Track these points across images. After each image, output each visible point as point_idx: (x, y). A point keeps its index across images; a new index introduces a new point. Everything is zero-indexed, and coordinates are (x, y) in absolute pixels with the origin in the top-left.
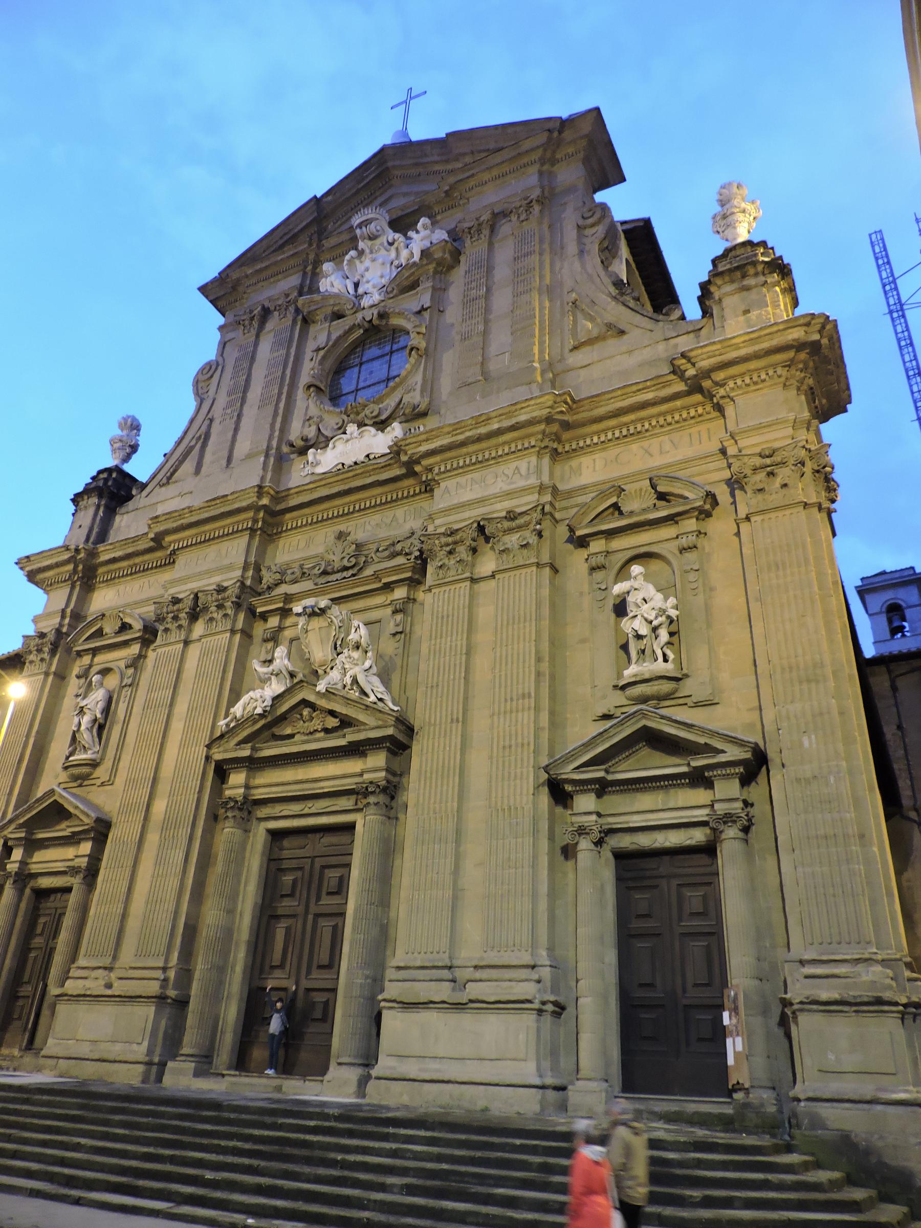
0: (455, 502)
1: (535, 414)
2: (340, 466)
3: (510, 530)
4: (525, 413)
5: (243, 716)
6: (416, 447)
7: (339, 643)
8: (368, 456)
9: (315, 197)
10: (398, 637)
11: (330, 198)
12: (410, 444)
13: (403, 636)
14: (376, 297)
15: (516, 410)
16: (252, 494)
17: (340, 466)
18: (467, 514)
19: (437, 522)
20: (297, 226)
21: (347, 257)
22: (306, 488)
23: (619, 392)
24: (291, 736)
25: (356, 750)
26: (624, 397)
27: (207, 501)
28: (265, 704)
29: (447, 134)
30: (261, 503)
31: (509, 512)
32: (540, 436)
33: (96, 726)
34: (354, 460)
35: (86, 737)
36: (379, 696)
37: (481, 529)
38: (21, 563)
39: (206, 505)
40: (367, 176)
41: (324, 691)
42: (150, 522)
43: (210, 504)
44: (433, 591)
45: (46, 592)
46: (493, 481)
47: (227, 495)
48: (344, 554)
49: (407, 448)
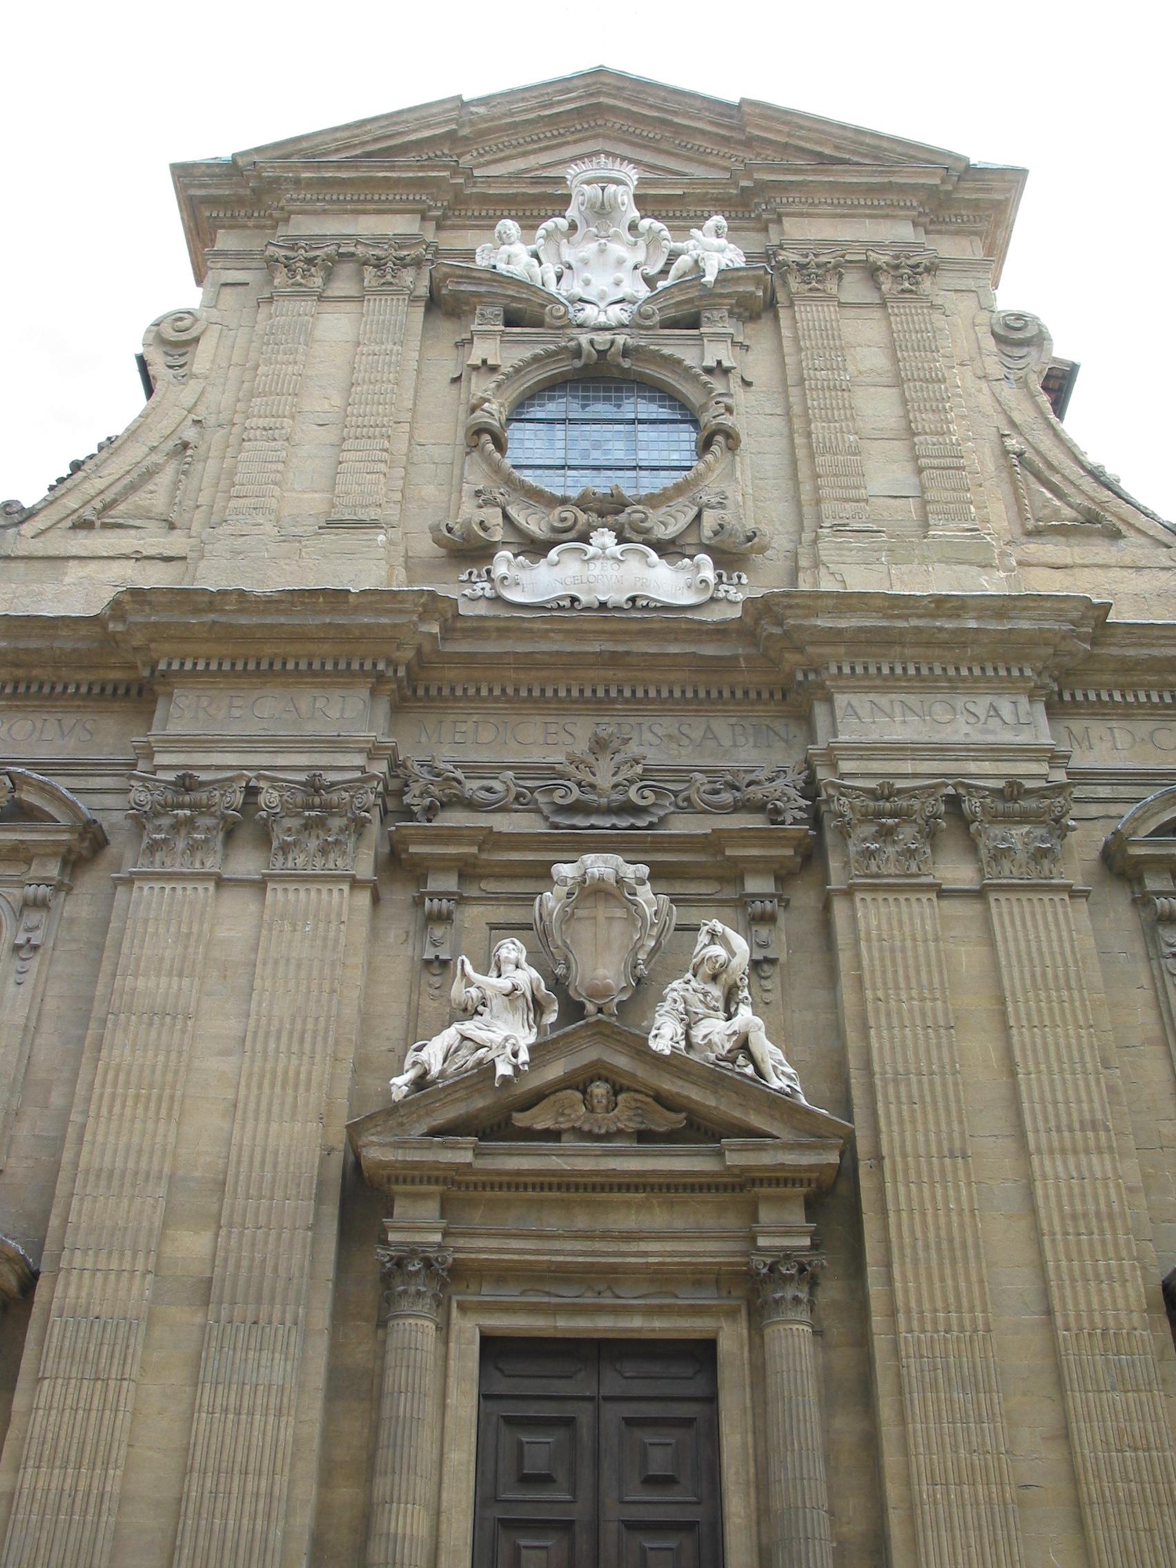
0: (874, 737)
2: (567, 603)
3: (1009, 819)
4: (1029, 619)
5: (442, 1074)
6: (807, 617)
7: (642, 956)
8: (633, 599)
9: (459, 97)
11: (482, 110)
12: (797, 606)
13: (778, 969)
14: (617, 314)
15: (1015, 608)
16: (409, 606)
17: (567, 603)
18: (908, 767)
21: (549, 224)
29: (743, 101)
30: (424, 628)
34: (602, 598)
37: (954, 802)
40: (560, 103)
42: (127, 598)
48: (619, 778)
49: (788, 612)
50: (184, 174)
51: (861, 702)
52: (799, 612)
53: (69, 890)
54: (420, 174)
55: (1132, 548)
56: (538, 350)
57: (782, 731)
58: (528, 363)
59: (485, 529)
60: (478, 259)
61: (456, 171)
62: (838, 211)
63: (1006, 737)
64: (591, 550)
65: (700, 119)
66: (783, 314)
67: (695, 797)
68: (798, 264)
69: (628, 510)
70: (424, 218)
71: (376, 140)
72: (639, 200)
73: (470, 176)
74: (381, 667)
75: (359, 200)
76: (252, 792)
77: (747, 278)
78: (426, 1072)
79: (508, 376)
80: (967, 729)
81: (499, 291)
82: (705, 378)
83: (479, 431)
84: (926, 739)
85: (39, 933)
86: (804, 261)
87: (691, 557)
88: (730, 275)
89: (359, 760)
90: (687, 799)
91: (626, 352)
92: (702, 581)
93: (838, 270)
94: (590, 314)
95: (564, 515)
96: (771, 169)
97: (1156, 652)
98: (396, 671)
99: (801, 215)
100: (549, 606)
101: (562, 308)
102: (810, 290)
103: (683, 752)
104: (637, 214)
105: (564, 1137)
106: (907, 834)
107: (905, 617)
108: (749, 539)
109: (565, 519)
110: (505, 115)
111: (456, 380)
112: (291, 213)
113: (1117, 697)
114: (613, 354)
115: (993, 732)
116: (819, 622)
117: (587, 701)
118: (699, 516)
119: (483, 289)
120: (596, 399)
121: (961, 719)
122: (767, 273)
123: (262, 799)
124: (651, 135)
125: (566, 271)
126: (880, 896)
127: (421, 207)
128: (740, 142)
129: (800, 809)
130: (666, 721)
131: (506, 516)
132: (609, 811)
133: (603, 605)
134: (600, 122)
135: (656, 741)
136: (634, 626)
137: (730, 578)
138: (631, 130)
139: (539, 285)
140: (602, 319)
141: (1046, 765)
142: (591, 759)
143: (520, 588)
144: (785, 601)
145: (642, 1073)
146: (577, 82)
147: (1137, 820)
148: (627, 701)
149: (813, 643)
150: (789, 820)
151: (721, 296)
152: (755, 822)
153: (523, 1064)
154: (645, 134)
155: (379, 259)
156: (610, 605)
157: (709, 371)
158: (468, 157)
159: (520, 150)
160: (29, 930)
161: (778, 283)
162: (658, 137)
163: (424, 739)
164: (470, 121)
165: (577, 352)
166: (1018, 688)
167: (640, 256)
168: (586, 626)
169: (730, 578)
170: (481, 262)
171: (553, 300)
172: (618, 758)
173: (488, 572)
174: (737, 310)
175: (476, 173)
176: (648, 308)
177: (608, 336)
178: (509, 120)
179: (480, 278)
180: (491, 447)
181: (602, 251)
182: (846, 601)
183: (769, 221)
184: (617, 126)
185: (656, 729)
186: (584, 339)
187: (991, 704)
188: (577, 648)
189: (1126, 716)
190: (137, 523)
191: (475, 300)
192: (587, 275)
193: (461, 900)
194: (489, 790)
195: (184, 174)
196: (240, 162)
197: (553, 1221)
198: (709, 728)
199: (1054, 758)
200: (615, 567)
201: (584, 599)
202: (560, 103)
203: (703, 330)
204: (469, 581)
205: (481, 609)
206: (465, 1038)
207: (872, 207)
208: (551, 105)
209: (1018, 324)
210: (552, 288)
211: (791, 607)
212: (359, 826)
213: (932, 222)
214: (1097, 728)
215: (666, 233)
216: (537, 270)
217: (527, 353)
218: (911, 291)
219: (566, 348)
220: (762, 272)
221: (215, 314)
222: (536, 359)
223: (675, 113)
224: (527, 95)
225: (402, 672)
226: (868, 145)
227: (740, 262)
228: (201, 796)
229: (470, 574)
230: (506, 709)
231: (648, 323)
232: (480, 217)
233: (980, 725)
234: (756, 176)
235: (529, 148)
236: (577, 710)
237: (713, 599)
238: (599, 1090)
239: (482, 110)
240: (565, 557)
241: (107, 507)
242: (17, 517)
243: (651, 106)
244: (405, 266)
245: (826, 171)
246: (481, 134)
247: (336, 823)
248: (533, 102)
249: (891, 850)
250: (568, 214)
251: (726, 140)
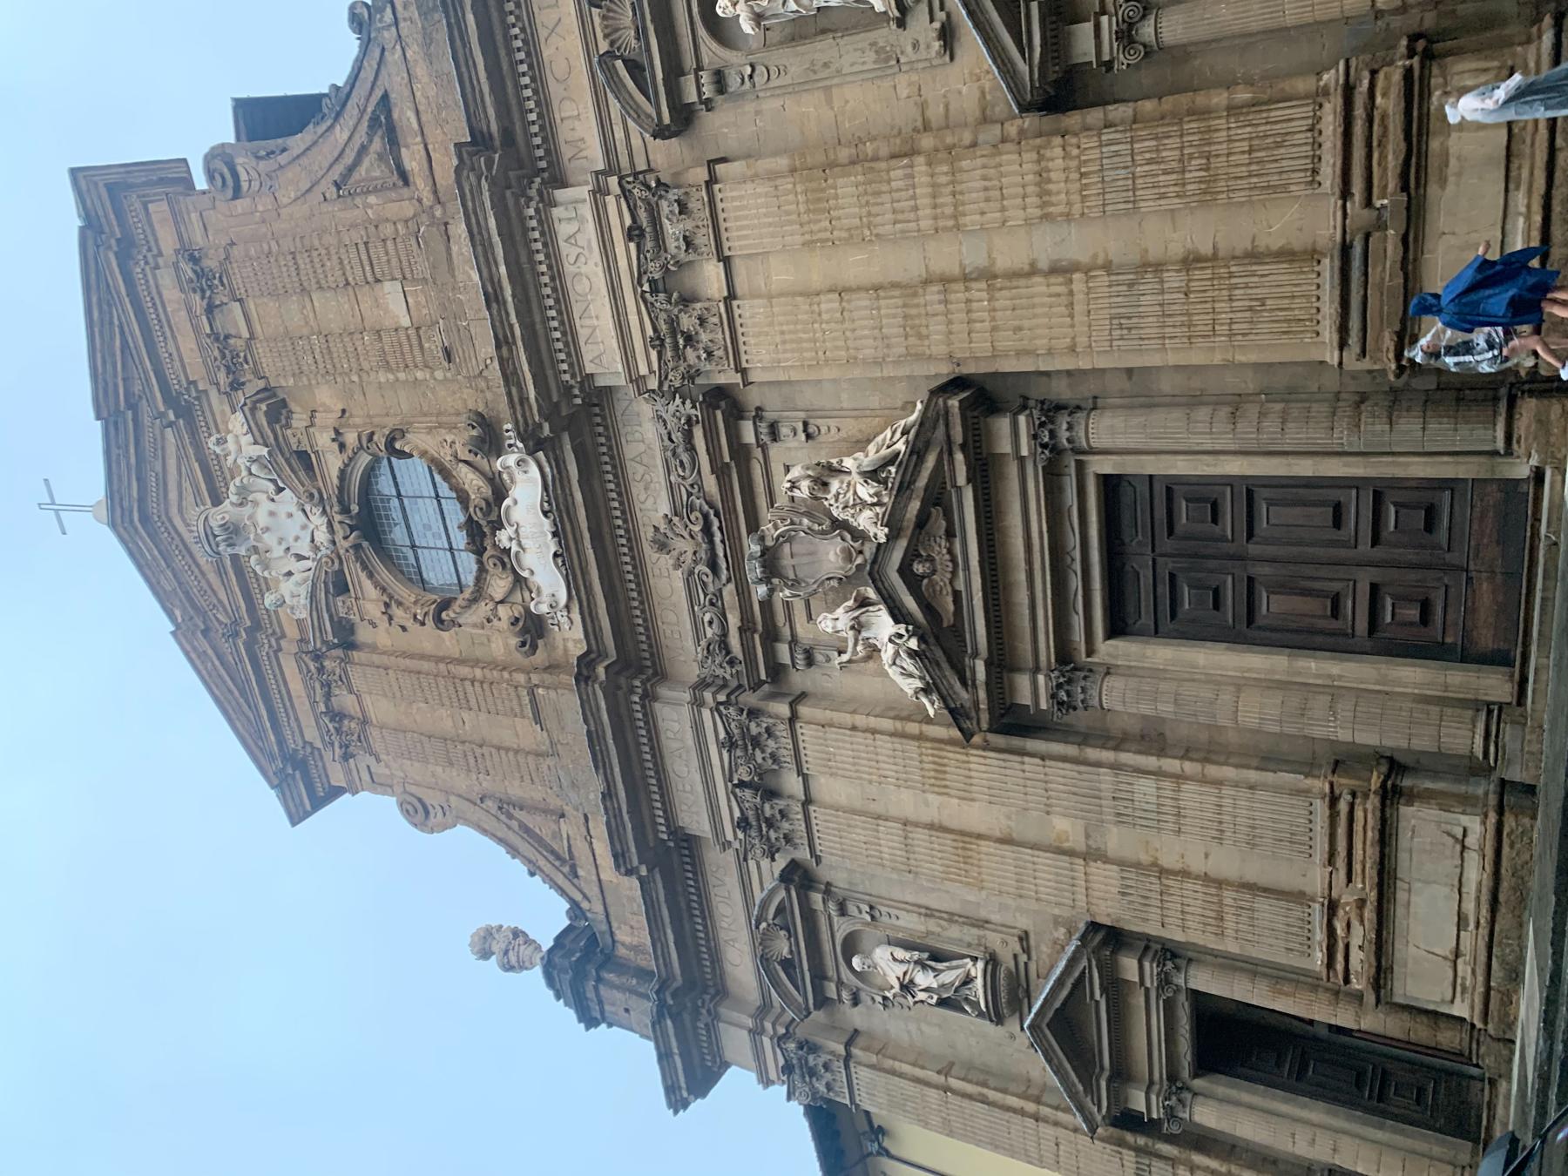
1: (488, 204)
2: (560, 561)
5: (922, 678)
7: (816, 527)
8: (545, 514)
10: (811, 429)
11: (178, 613)
13: (811, 421)
14: (318, 520)
18: (633, 319)
19: (643, 370)
21: (258, 569)
22: (585, 604)
23: (464, 69)
24: (957, 595)
25: (985, 471)
26: (471, 63)
27: (596, 767)
28: (903, 632)
29: (98, 417)
31: (631, 239)
32: (522, 200)
33: (932, 963)
34: (550, 536)
35: (950, 976)
36: (898, 435)
38: (677, 1102)
39: (601, 771)
41: (886, 530)
43: (601, 764)
44: (744, 365)
45: (725, 1065)
46: (585, 280)
47: (589, 732)
50: (297, 816)
51: (588, 353)
53: (828, 884)
55: (394, 80)
56: (363, 576)
57: (625, 404)
59: (517, 620)
62: (168, 334)
63: (590, 227)
64: (515, 548)
67: (690, 481)
68: (228, 374)
72: (217, 501)
74: (636, 699)
76: (742, 784)
78: (922, 689)
79: (391, 597)
80: (591, 263)
81: (323, 602)
84: (607, 299)
85: (862, 906)
89: (706, 713)
90: (692, 486)
91: (345, 510)
93: (221, 339)
94: (322, 536)
97: (486, 89)
103: (655, 480)
104: (227, 501)
105: (958, 588)
106: (687, 322)
107: (511, 326)
112: (305, 742)
113: (533, 117)
115: (589, 241)
120: (387, 517)
121: (584, 269)
123: (746, 778)
125: (293, 551)
126: (742, 348)
127: (272, 654)
129: (683, 403)
130: (635, 491)
132: (711, 542)
133: (555, 534)
135: (651, 500)
140: (324, 528)
141: (608, 198)
142: (675, 553)
145: (902, 544)
147: (638, 115)
149: (550, 398)
150: (693, 412)
151: (276, 438)
152: (698, 433)
153: (907, 631)
160: (860, 912)
163: (682, 659)
165: (357, 547)
166: (547, 218)
167: (262, 497)
170: (303, 614)
172: (670, 534)
174: (284, 422)
177: (337, 526)
181: (267, 529)
182: (510, 376)
183: (197, 391)
185: (642, 499)
187: (566, 241)
189: (548, 104)
190: (565, 836)
191: (336, 619)
192: (291, 539)
193: (794, 641)
194: (711, 623)
195: (297, 816)
196: (276, 782)
197: (1021, 596)
198: (632, 460)
199: (599, 192)
201: (553, 548)
205: (576, 617)
206: (894, 663)
209: (217, 177)
212: (754, 713)
213: (150, 250)
214: (564, 133)
215: (237, 481)
216: (297, 577)
217: (367, 584)
218: (220, 277)
220: (246, 408)
221: (398, 789)
222: (371, 576)
228: (750, 814)
233: (586, 252)
234: (162, 409)
238: (919, 568)
239: (178, 613)
241: (558, 857)
242: (578, 912)
244: (323, 667)
247: (754, 730)
249: (704, 337)
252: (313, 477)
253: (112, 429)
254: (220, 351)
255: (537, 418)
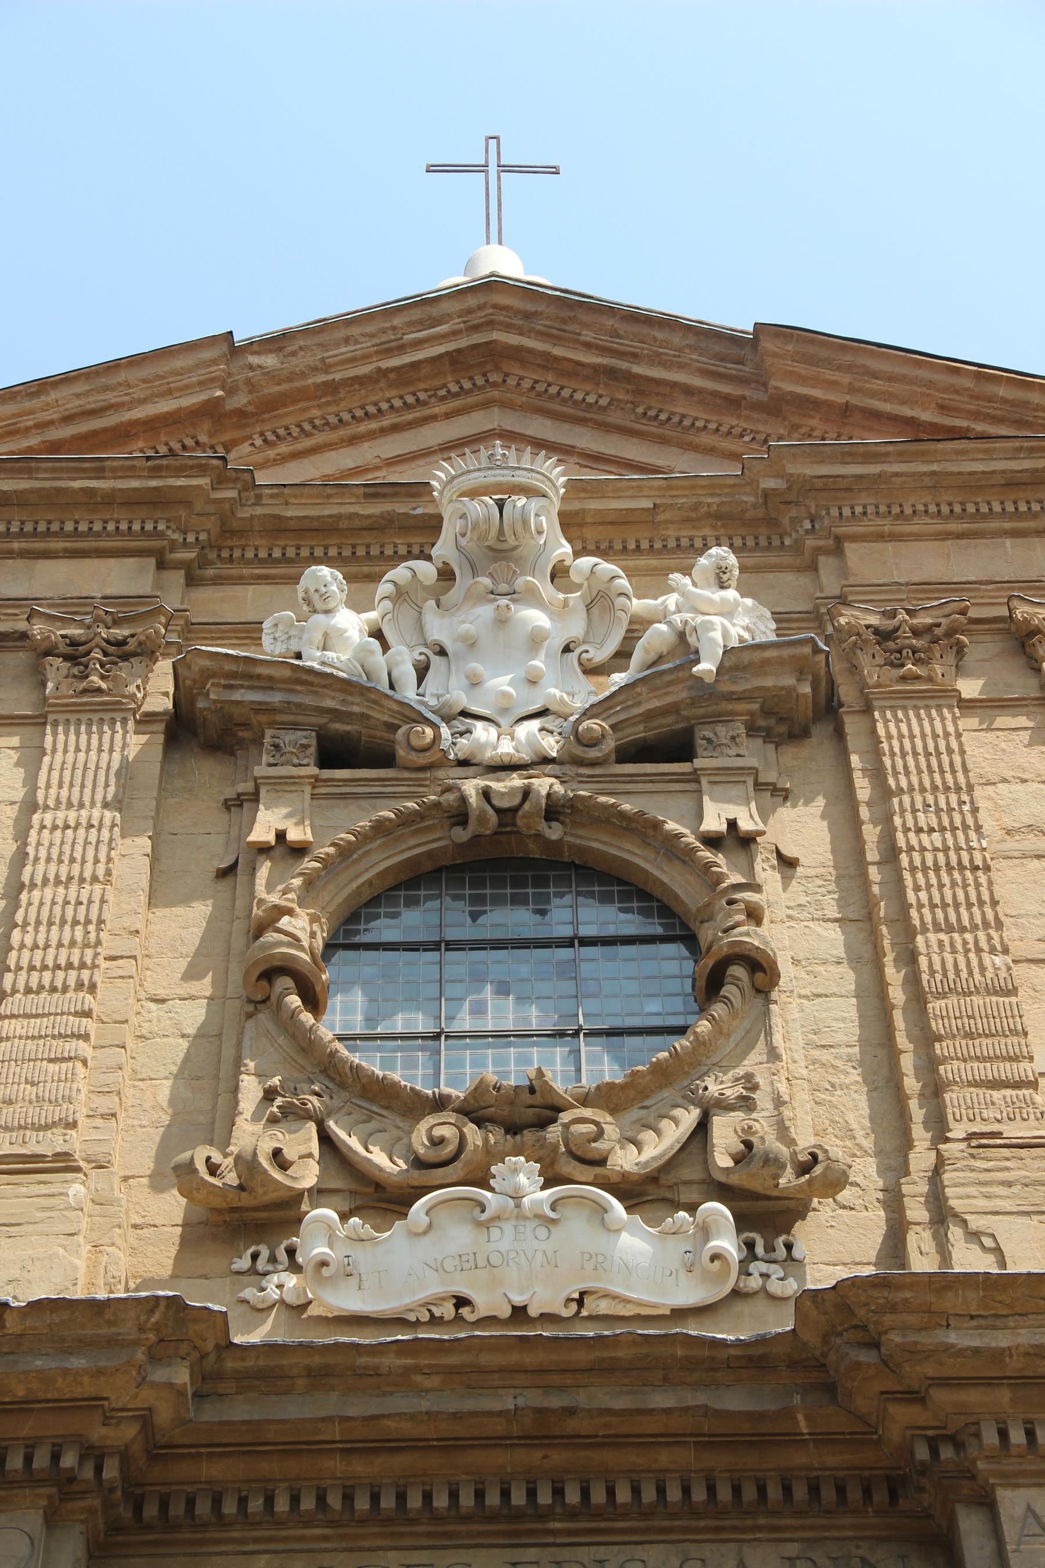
2: (448, 1310)
11: (270, 361)
16: (128, 1329)
17: (448, 1310)
20: (130, 405)
21: (400, 573)
29: (760, 328)
34: (518, 1299)
40: (418, 344)
49: (888, 1319)
52: (912, 1319)
54: (154, 483)
58: (364, 838)
60: (266, 640)
61: (221, 479)
62: (953, 526)
65: (681, 366)
66: (852, 725)
68: (877, 631)
69: (565, 1117)
70: (161, 566)
71: (68, 419)
73: (245, 481)
75: (35, 533)
77: (781, 662)
79: (326, 862)
81: (308, 700)
82: (706, 854)
83: (271, 973)
86: (889, 624)
87: (692, 1208)
88: (746, 658)
91: (553, 810)
92: (714, 1258)
95: (438, 1132)
96: (818, 454)
98: (99, 1469)
99: (881, 537)
100: (412, 1317)
101: (429, 731)
102: (904, 679)
104: (567, 548)
108: (804, 1169)
109: (441, 1141)
110: (315, 369)
111: (227, 872)
114: (524, 816)
116: (952, 1338)
117: (491, 1517)
118: (702, 1128)
119: (276, 698)
120: (498, 901)
122: (817, 650)
124: (591, 399)
125: (435, 660)
128: (757, 406)
131: (326, 1139)
133: (519, 1313)
134: (494, 377)
136: (582, 1357)
137: (770, 1248)
138: (553, 390)
139: (384, 686)
140: (506, 748)
143: (353, 1281)
144: (881, 1296)
146: (446, 307)
148: (573, 1514)
149: (944, 1382)
151: (730, 697)
154: (578, 396)
155: (74, 643)
156: (533, 1312)
157: (713, 841)
158: (245, 448)
159: (343, 432)
161: (838, 667)
162: (604, 402)
164: (248, 381)
165: (460, 815)
167: (576, 629)
168: (486, 1359)
169: (770, 1248)
171: (414, 717)
173: (291, 1252)
175: (262, 478)
176: (594, 725)
177: (516, 781)
178: (322, 378)
179: (270, 678)
180: (294, 1001)
183: (818, 551)
184: (527, 384)
186: (471, 787)
188: (468, 1405)
191: (263, 718)
192: (476, 666)
200: (542, 1232)
202: (418, 344)
203: (698, 763)
204: (253, 1271)
207: (1017, 515)
208: (402, 349)
210: (409, 693)
211: (893, 1308)
215: (624, 582)
216: (379, 660)
219: (437, 805)
220: (807, 650)
222: (380, 828)
223: (634, 357)
224: (355, 331)
225: (111, 1471)
226: (1004, 401)
227: (767, 632)
229: (255, 1257)
230: (325, 1538)
231: (593, 754)
232: (270, 560)
234: (791, 469)
235: (363, 428)
236: (469, 1535)
237: (736, 1294)
240: (442, 1216)
243: (588, 346)
244: (125, 657)
245: (924, 453)
246: (271, 405)
248: (366, 346)
250: (435, 552)
251: (733, 403)
252: (625, 754)
253: (733, 351)
254: (929, 628)
255: (896, 1338)
